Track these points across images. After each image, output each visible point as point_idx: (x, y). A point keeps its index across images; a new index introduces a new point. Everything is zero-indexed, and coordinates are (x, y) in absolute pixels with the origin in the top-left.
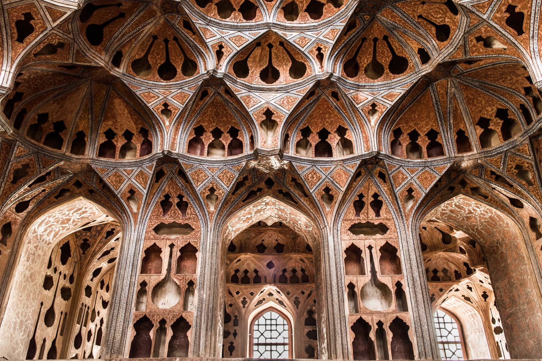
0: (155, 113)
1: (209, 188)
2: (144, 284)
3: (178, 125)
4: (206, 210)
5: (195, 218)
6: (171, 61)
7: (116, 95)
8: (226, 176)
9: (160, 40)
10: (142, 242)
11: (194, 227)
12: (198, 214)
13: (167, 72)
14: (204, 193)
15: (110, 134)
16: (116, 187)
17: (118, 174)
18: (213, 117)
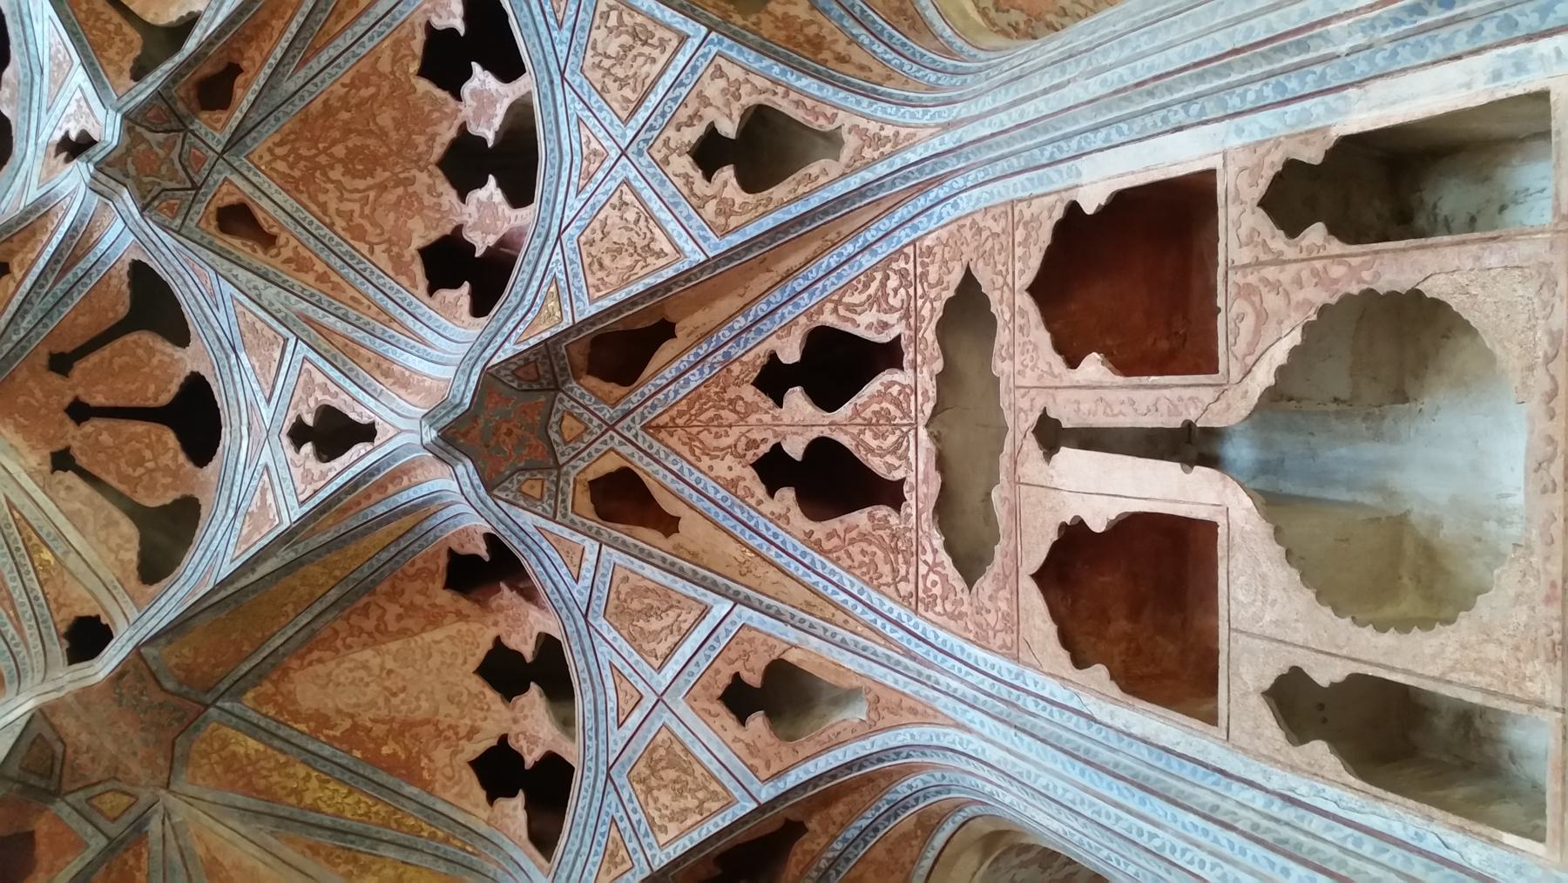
0: (323, 495)
1: (697, 175)
2: (1298, 704)
3: (387, 374)
4: (840, 189)
5: (903, 274)
6: (165, 399)
7: (267, 687)
8: (619, 60)
9: (75, 436)
10: (1031, 679)
11: (956, 277)
12: (884, 249)
13: (195, 419)
14: (725, 209)
15: (499, 770)
16: (714, 796)
17: (642, 769)
18: (383, 188)
